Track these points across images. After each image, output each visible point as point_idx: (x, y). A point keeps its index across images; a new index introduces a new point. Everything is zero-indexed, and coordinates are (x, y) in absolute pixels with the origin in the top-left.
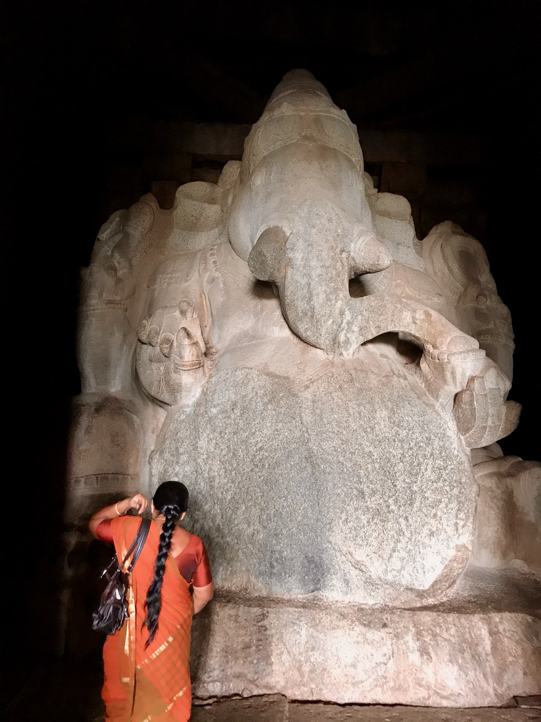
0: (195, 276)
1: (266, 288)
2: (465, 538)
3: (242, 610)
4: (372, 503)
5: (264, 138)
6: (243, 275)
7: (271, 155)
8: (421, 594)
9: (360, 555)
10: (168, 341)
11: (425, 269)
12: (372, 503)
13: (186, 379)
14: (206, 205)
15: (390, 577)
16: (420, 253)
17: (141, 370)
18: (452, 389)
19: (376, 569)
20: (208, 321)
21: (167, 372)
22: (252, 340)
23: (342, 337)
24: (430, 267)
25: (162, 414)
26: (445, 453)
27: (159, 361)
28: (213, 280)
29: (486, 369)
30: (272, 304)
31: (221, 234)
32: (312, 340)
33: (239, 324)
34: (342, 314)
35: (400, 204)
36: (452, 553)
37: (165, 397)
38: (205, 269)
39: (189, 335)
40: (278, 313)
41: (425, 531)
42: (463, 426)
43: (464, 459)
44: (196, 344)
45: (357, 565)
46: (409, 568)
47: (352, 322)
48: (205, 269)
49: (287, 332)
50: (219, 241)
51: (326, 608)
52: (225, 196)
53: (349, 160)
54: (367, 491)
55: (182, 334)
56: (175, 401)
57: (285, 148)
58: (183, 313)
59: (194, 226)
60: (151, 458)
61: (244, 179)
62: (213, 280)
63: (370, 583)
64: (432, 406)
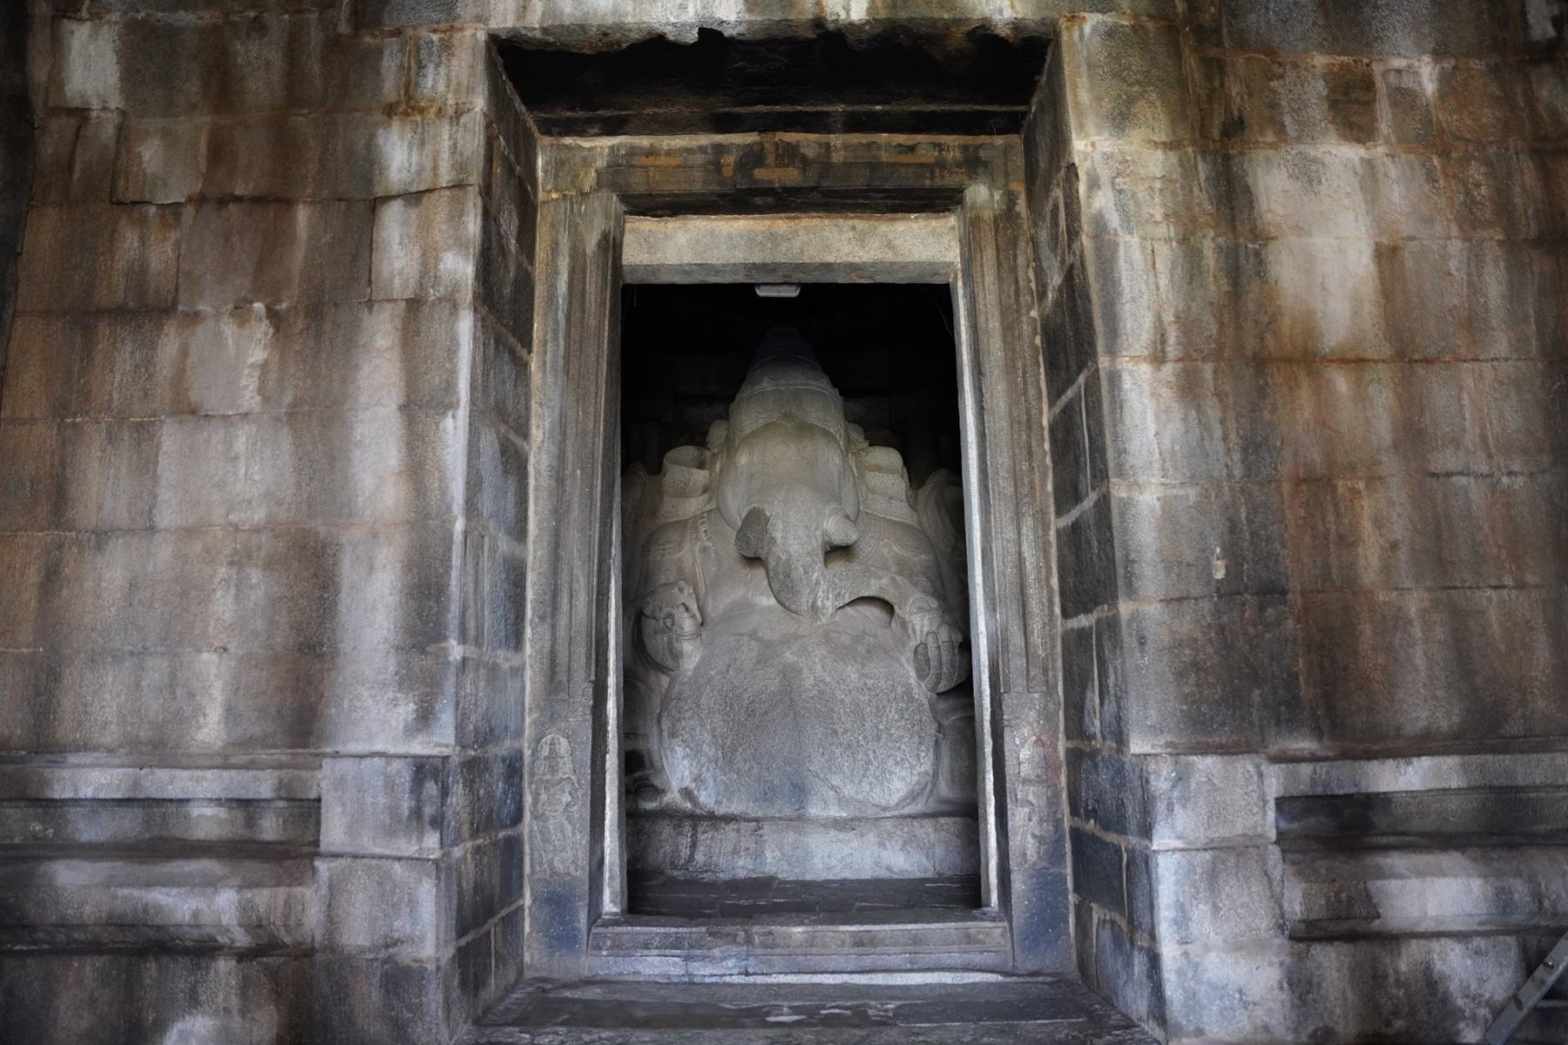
0: (687, 547)
1: (754, 561)
2: (926, 765)
3: (743, 825)
4: (845, 739)
5: (750, 415)
6: (730, 550)
7: (753, 435)
8: (885, 809)
9: (836, 780)
10: (670, 616)
11: (920, 523)
12: (845, 739)
13: (687, 647)
14: (695, 470)
15: (860, 797)
16: (913, 506)
17: (646, 641)
18: (913, 644)
19: (849, 790)
20: (702, 589)
21: (670, 642)
22: (745, 607)
23: (819, 603)
24: (924, 520)
25: (665, 680)
26: (908, 696)
27: (662, 632)
28: (704, 549)
29: (939, 626)
30: (760, 572)
31: (710, 500)
32: (793, 607)
33: (729, 596)
34: (818, 583)
35: (889, 458)
36: (915, 778)
37: (669, 663)
38: (697, 539)
39: (687, 609)
40: (765, 583)
41: (891, 761)
42: (921, 676)
43: (925, 702)
44: (693, 616)
45: (833, 788)
46: (878, 790)
47: (827, 590)
48: (697, 539)
49: (773, 601)
50: (708, 508)
51: (810, 821)
52: (713, 464)
53: (827, 434)
54: (840, 730)
55: (682, 609)
56: (678, 666)
57: (767, 427)
58: (681, 590)
59: (683, 494)
60: (660, 716)
61: (730, 448)
62: (704, 549)
63: (842, 801)
64: (898, 660)
